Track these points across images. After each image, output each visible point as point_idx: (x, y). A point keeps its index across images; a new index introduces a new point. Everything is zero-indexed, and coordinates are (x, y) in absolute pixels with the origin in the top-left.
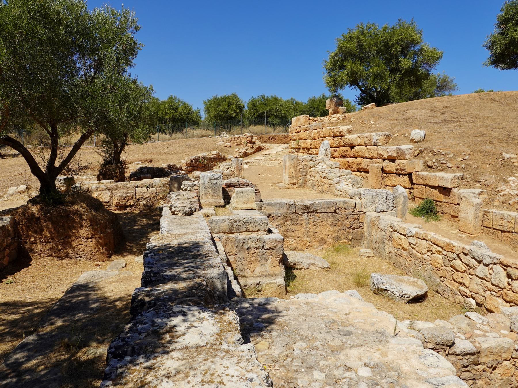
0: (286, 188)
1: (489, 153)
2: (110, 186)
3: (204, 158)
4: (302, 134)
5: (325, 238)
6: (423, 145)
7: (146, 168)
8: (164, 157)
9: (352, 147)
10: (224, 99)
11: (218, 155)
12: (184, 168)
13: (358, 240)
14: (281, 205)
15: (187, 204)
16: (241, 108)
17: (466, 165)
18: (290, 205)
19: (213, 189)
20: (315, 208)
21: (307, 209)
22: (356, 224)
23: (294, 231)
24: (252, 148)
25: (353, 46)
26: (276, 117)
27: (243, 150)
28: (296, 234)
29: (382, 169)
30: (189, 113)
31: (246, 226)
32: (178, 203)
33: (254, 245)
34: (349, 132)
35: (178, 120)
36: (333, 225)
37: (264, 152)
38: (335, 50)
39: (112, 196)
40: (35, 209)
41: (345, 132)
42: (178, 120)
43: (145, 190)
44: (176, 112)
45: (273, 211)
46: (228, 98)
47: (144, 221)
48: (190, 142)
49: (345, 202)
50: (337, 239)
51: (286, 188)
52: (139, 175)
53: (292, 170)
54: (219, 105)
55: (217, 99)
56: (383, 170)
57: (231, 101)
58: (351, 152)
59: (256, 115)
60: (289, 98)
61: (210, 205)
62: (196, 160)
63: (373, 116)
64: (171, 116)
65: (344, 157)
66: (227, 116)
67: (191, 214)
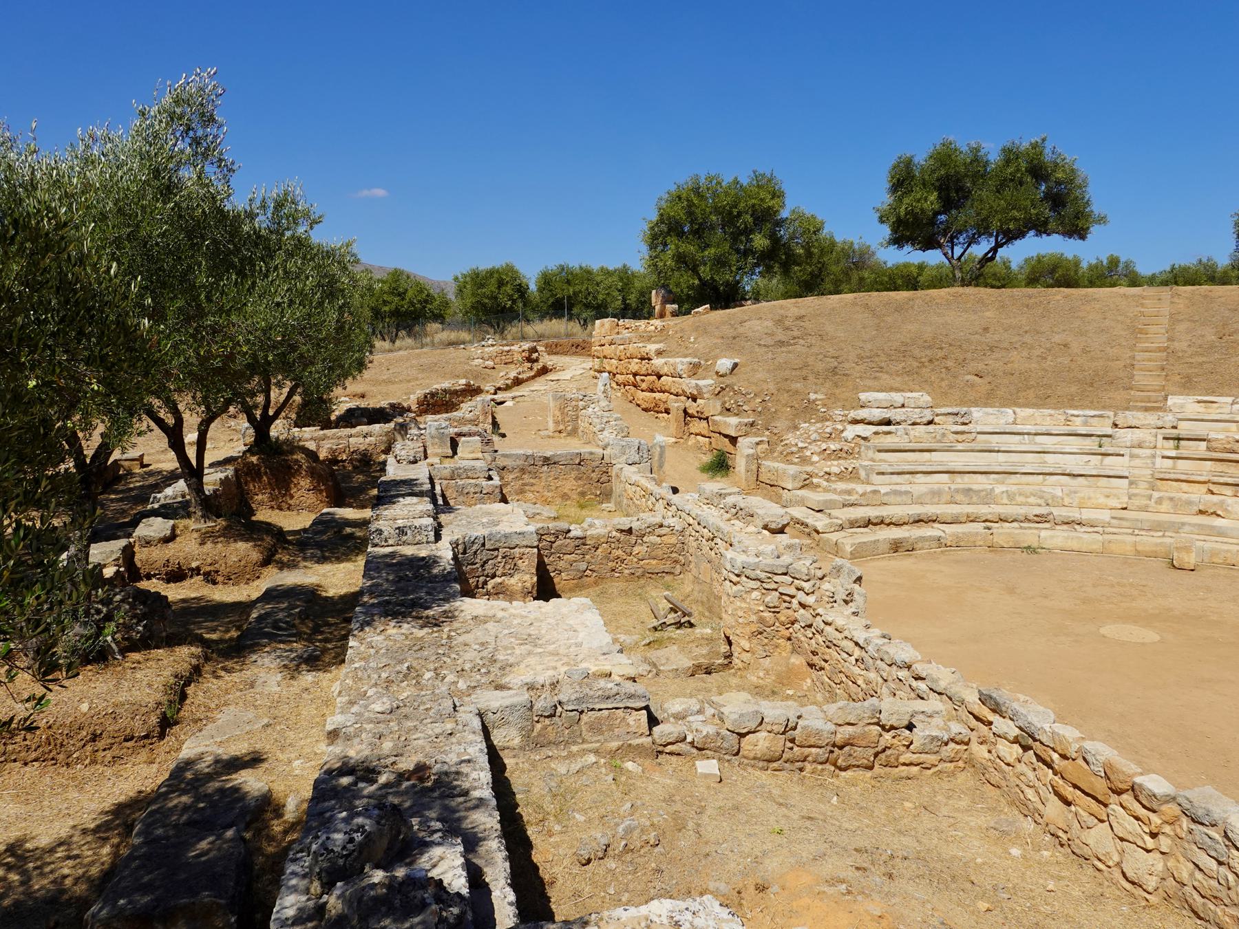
0: (549, 437)
1: (797, 392)
2: (316, 434)
3: (445, 391)
4: (608, 350)
5: (569, 493)
6: (728, 380)
7: (358, 408)
8: (384, 389)
9: (659, 377)
10: (491, 273)
11: (468, 385)
12: (414, 407)
13: (607, 495)
14: (518, 456)
15: (412, 453)
16: (522, 290)
17: (764, 408)
18: (527, 457)
19: (440, 439)
20: (556, 459)
21: (547, 461)
22: (604, 478)
23: (532, 485)
24: (531, 369)
25: (679, 212)
26: (587, 306)
27: (513, 374)
28: (535, 488)
29: (685, 411)
30: (426, 301)
31: (468, 473)
32: (403, 453)
33: (472, 490)
34: (659, 353)
35: (408, 311)
36: (578, 479)
37: (550, 376)
38: (655, 217)
39: (318, 447)
40: (254, 459)
41: (652, 354)
42: (408, 311)
43: (361, 440)
44: (403, 299)
45: (508, 463)
46: (498, 271)
47: (361, 478)
48: (427, 355)
49: (591, 453)
50: (583, 494)
51: (549, 437)
52: (352, 418)
53: (558, 413)
54: (482, 286)
55: (477, 275)
56: (685, 411)
57: (504, 279)
58: (658, 384)
59: (551, 300)
60: (619, 265)
61: (436, 455)
62: (433, 395)
63: (696, 329)
64: (393, 307)
65: (652, 391)
66: (496, 304)
67: (415, 462)
